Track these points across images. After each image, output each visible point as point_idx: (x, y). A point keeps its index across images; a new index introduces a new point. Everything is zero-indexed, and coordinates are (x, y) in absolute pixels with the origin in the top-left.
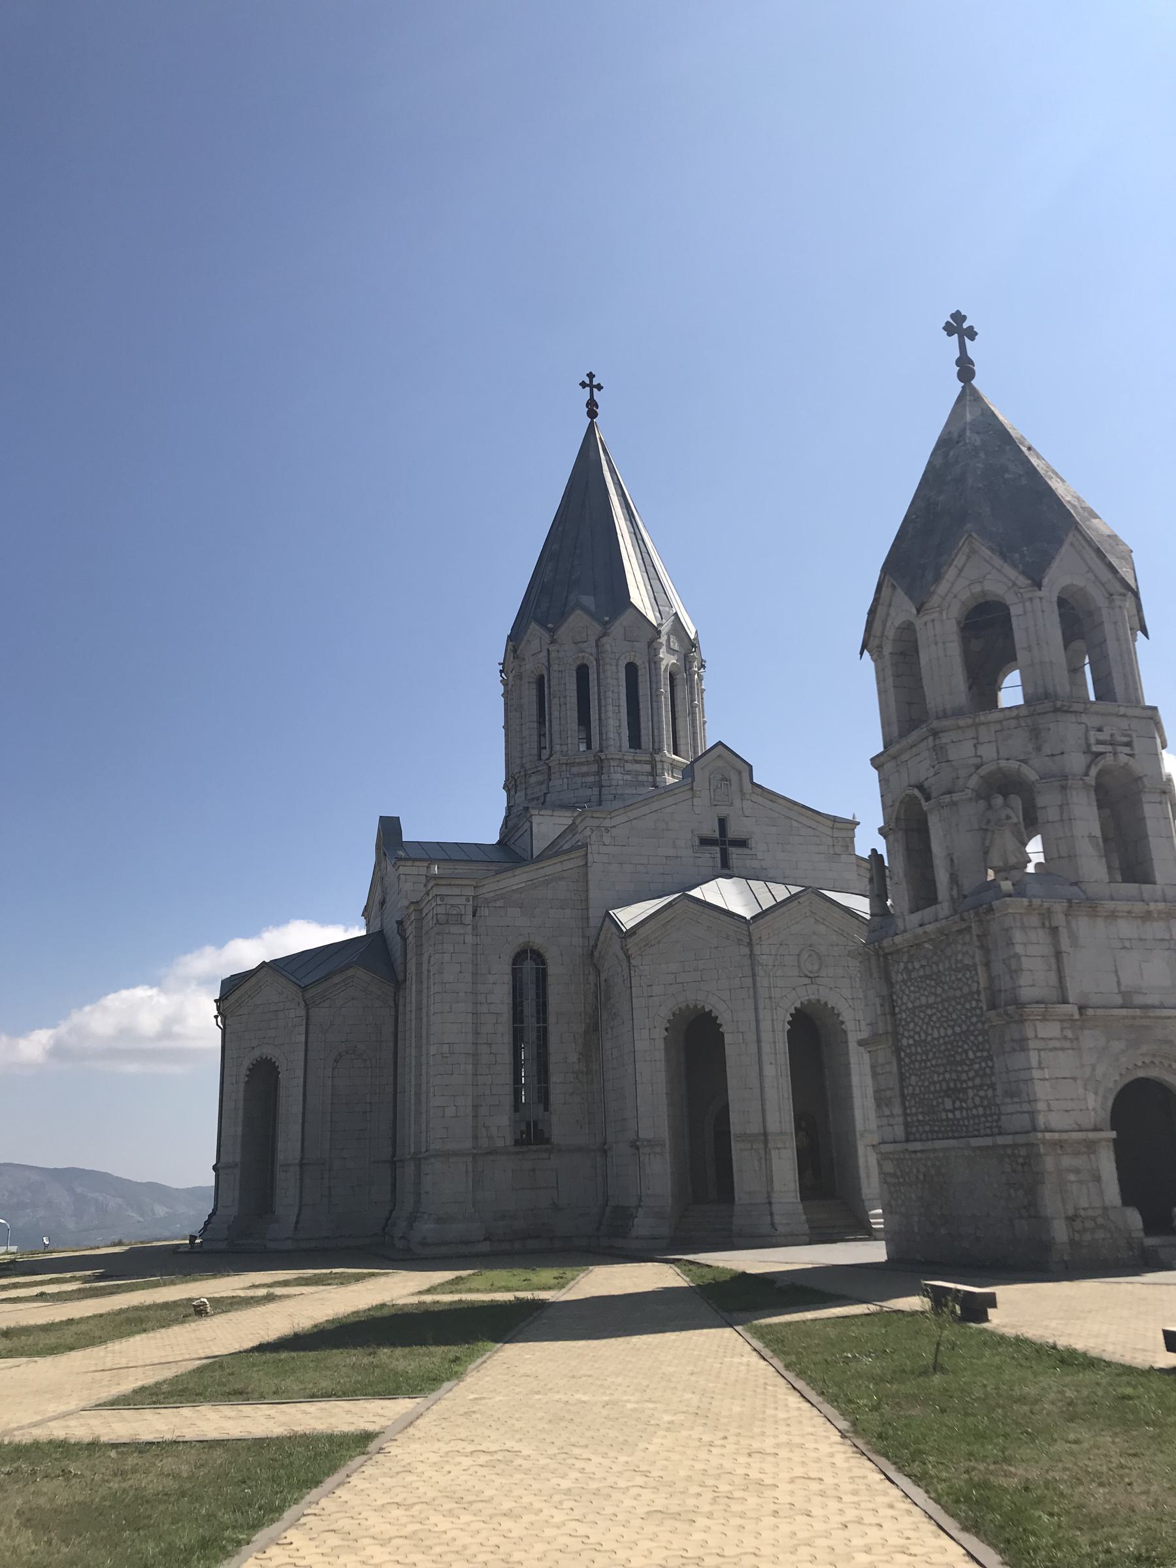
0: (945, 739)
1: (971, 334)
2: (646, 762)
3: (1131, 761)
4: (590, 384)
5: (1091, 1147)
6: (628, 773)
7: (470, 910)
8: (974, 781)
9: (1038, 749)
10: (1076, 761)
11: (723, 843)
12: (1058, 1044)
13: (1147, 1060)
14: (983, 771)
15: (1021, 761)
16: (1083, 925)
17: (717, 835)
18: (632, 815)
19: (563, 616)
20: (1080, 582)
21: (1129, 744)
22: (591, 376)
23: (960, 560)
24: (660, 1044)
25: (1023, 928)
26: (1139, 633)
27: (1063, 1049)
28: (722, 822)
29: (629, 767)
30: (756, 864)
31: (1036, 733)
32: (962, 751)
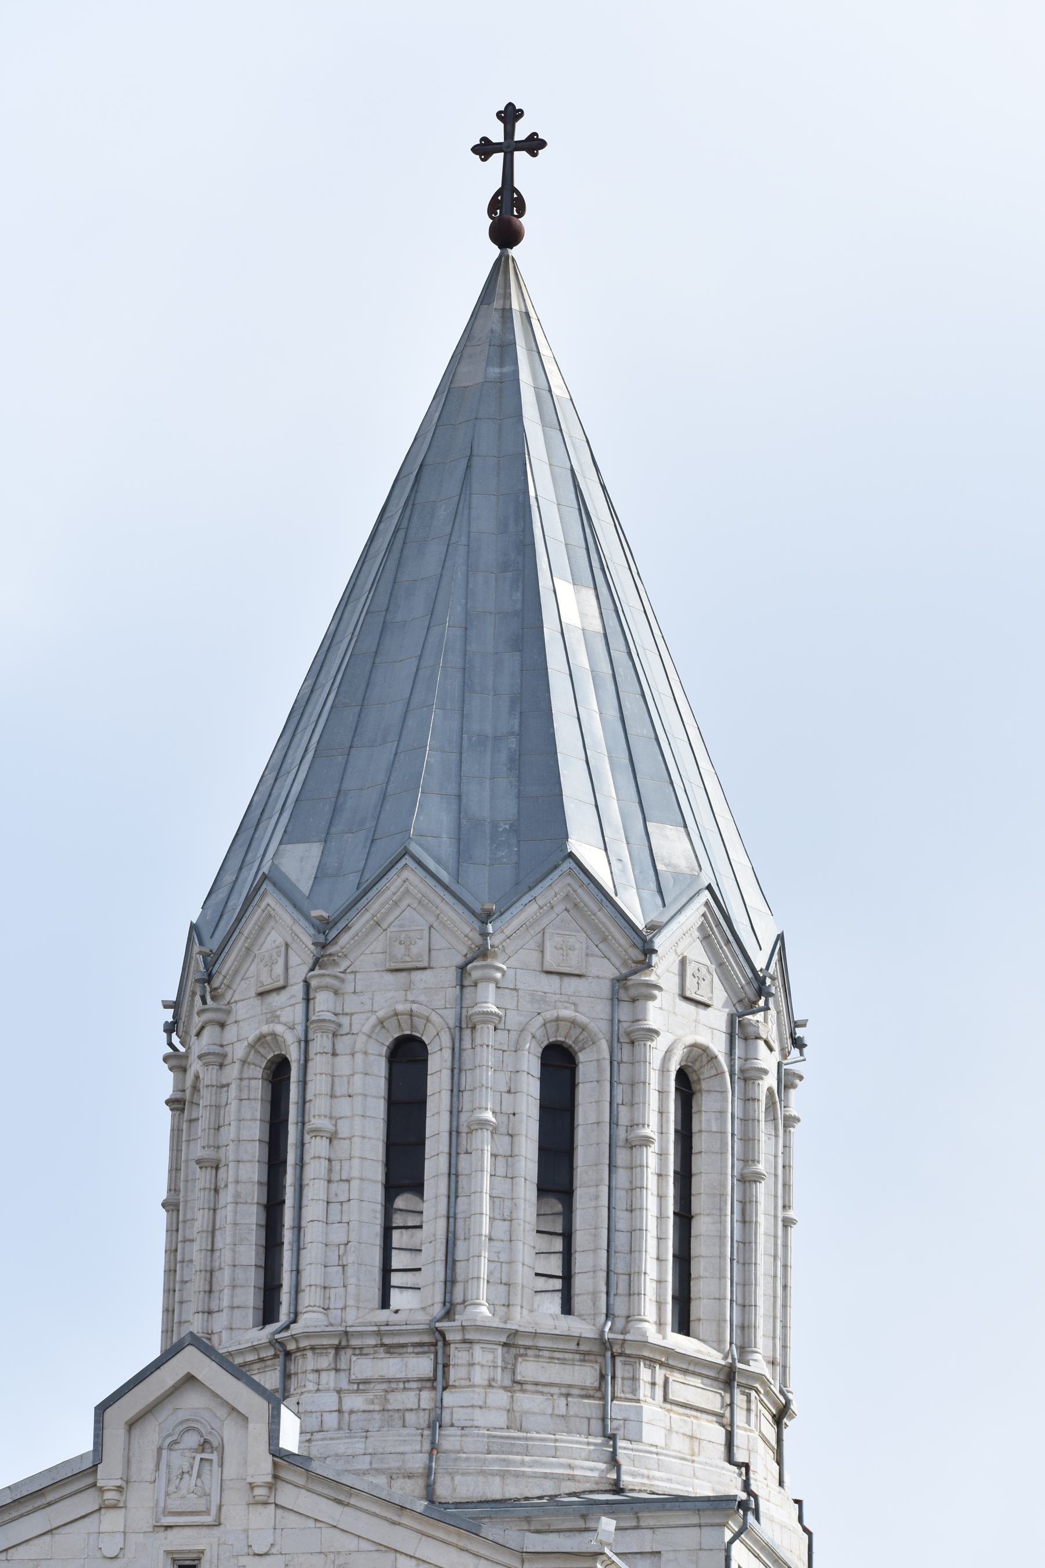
4: (510, 140)
6: (362, 1384)
22: (510, 115)
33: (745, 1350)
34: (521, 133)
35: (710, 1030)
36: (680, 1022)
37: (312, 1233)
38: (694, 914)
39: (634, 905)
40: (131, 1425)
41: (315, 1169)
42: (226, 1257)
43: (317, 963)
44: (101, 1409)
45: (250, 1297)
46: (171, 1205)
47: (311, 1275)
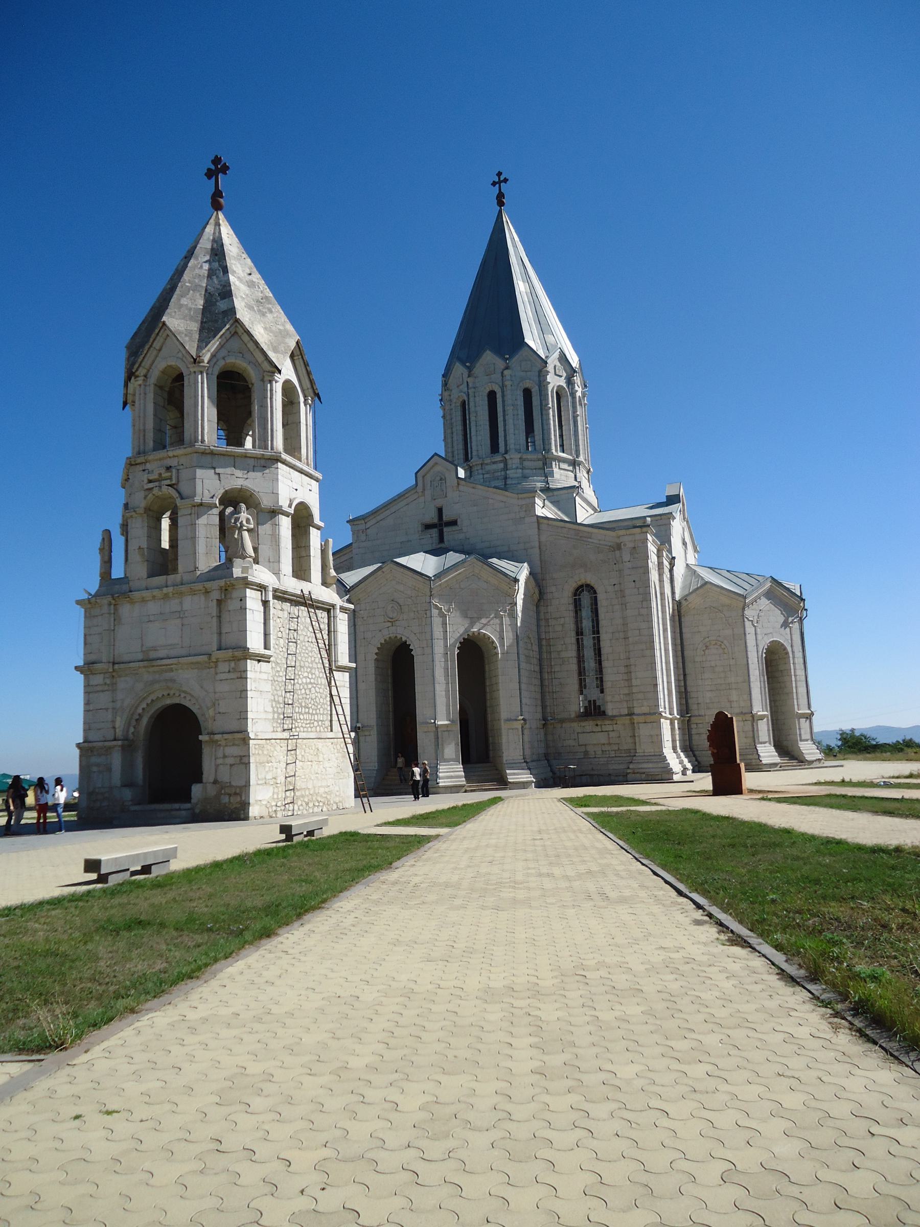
1: (224, 170)
2: (501, 462)
4: (500, 180)
5: (108, 751)
11: (441, 525)
12: (99, 688)
13: (165, 693)
16: (125, 610)
17: (436, 521)
18: (379, 518)
20: (172, 362)
21: (171, 479)
27: (103, 691)
28: (440, 511)
29: (488, 468)
30: (461, 536)
33: (578, 456)
34: (502, 179)
35: (562, 382)
36: (555, 381)
37: (474, 438)
38: (556, 354)
39: (542, 354)
40: (423, 477)
41: (473, 424)
42: (456, 448)
43: (469, 376)
44: (416, 473)
45: (462, 456)
46: (445, 440)
47: (474, 448)
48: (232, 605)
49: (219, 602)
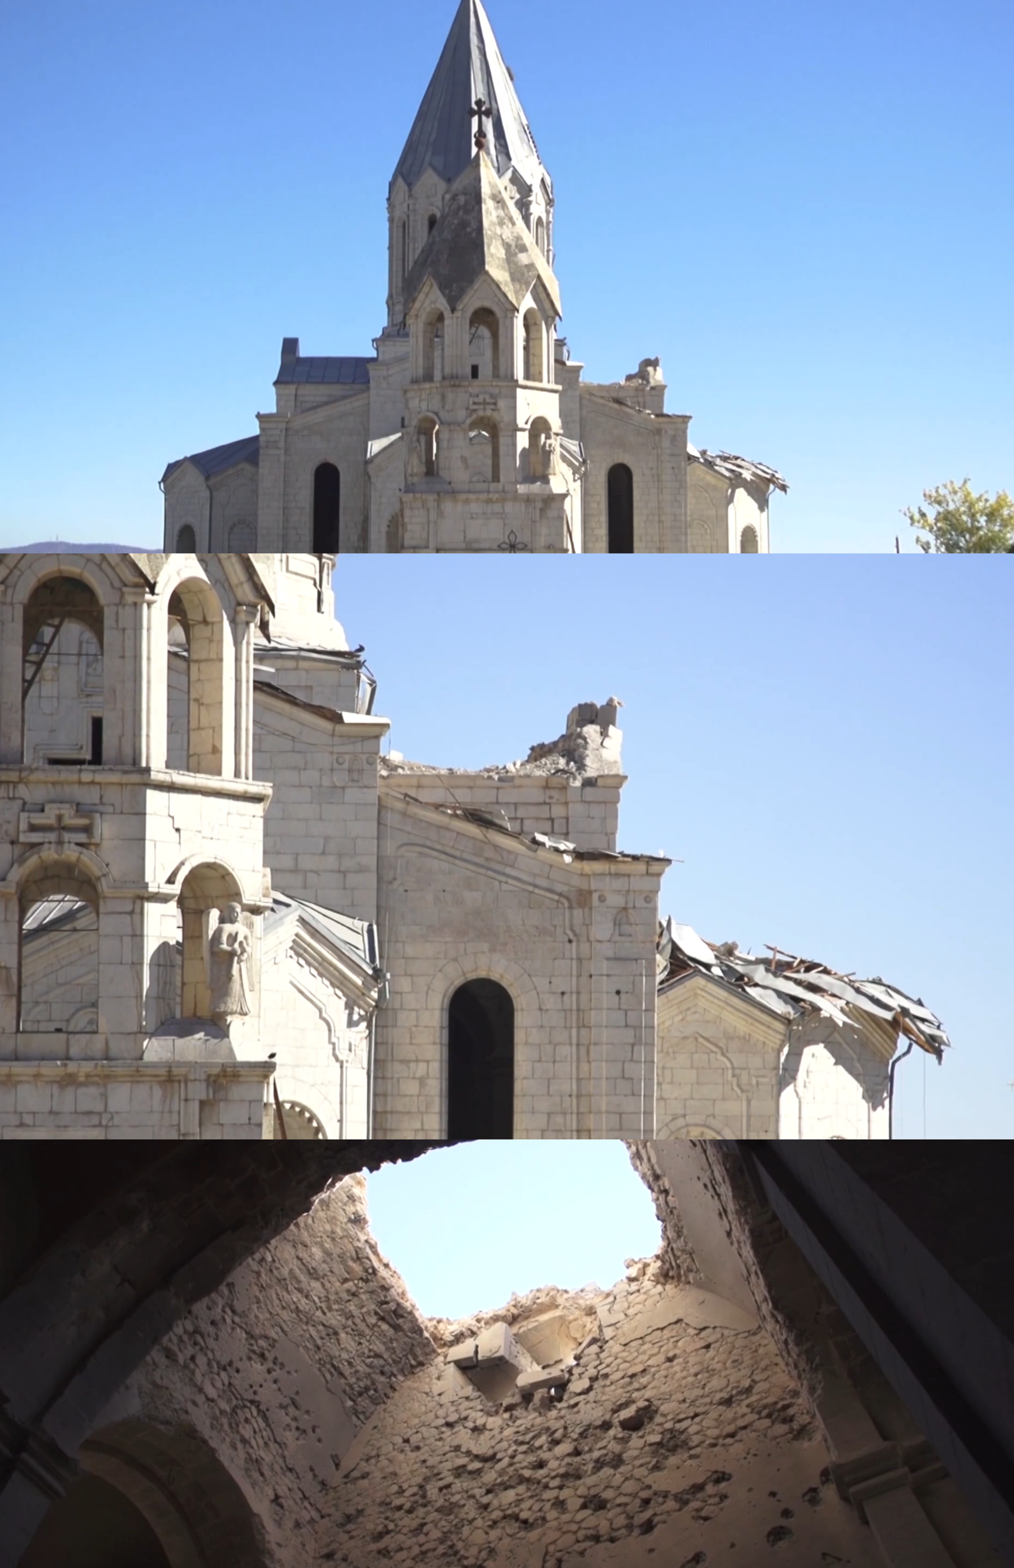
0: (409, 395)
3: (495, 415)
7: (283, 439)
8: (415, 422)
9: (443, 406)
10: (461, 414)
14: (421, 416)
15: (436, 414)
16: (448, 506)
19: (419, 174)
20: (487, 304)
23: (426, 289)
24: (384, 536)
25: (411, 508)
26: (557, 318)
31: (443, 397)
32: (414, 404)
48: (551, 513)
49: (541, 510)
